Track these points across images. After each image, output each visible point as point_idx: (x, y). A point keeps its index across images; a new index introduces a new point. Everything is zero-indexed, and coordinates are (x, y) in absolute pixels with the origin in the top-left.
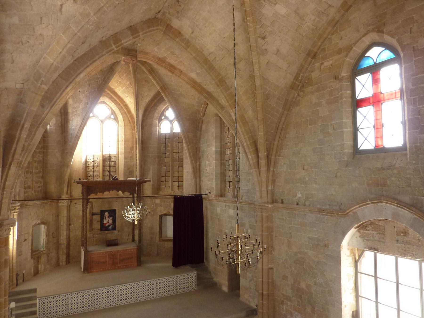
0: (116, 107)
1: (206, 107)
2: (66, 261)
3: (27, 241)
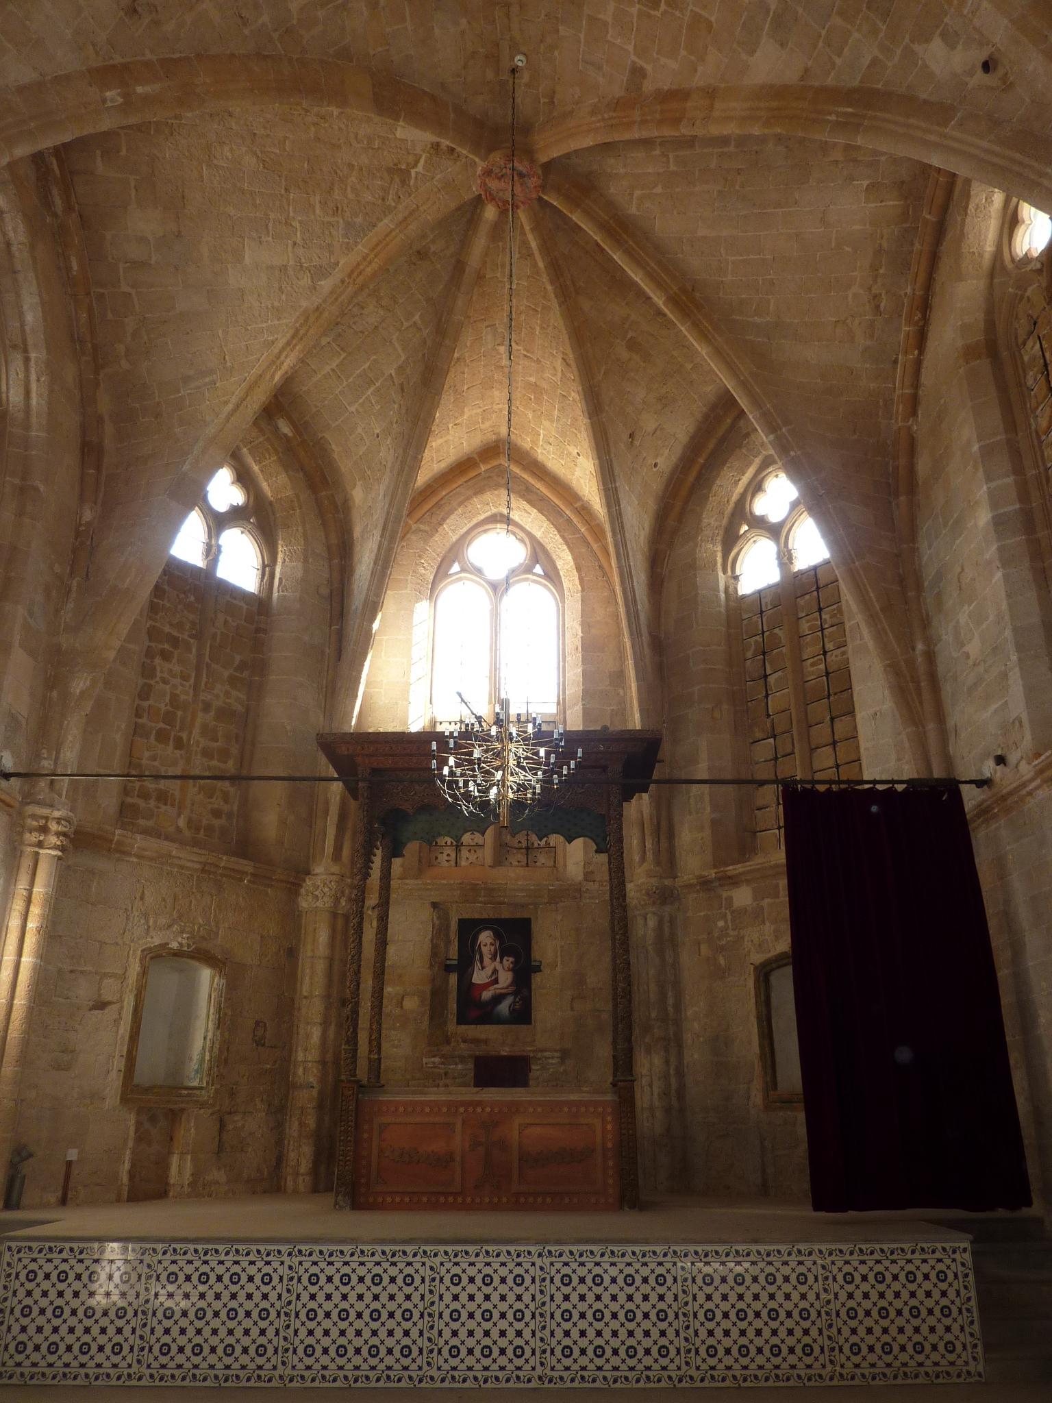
0: (546, 524)
1: (918, 363)
3: (111, 1012)
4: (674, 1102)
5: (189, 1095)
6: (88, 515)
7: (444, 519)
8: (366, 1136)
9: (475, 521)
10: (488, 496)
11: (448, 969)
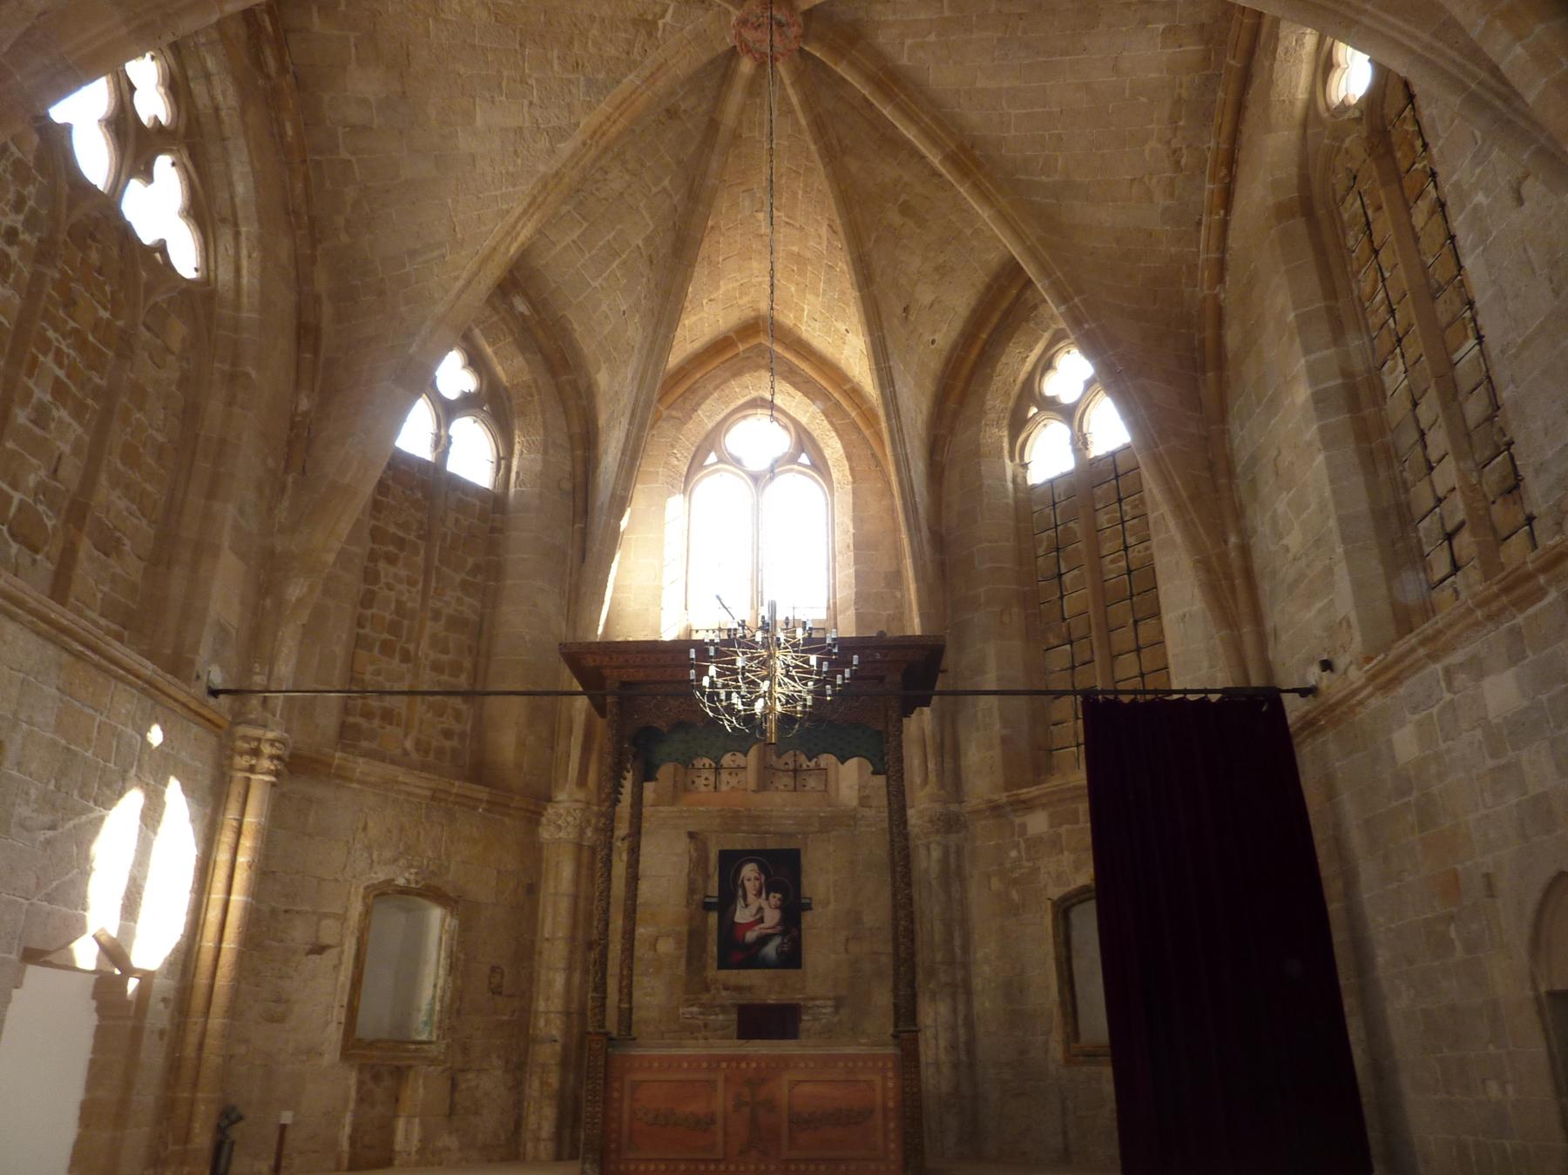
1: (1224, 225)
2: (558, 1137)
3: (329, 958)
4: (963, 1058)
5: (416, 1050)
6: (304, 404)
7: (699, 405)
8: (616, 1095)
9: (732, 406)
10: (747, 378)
11: (707, 907)
